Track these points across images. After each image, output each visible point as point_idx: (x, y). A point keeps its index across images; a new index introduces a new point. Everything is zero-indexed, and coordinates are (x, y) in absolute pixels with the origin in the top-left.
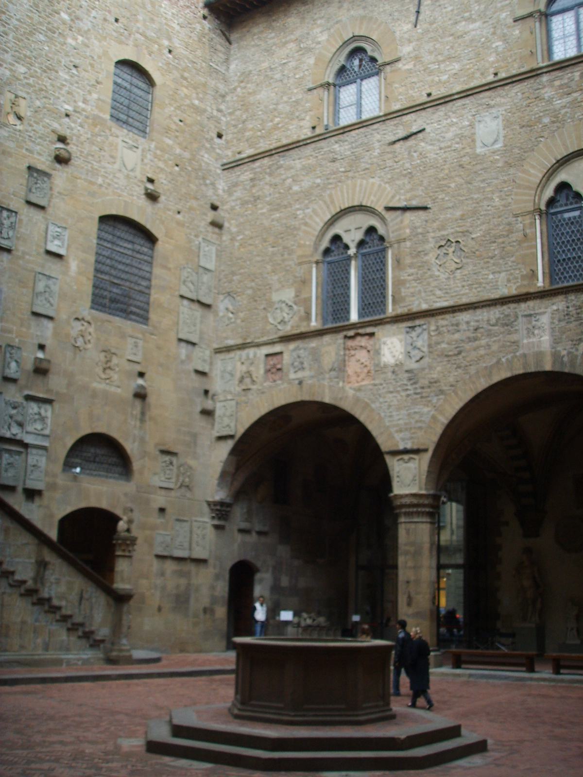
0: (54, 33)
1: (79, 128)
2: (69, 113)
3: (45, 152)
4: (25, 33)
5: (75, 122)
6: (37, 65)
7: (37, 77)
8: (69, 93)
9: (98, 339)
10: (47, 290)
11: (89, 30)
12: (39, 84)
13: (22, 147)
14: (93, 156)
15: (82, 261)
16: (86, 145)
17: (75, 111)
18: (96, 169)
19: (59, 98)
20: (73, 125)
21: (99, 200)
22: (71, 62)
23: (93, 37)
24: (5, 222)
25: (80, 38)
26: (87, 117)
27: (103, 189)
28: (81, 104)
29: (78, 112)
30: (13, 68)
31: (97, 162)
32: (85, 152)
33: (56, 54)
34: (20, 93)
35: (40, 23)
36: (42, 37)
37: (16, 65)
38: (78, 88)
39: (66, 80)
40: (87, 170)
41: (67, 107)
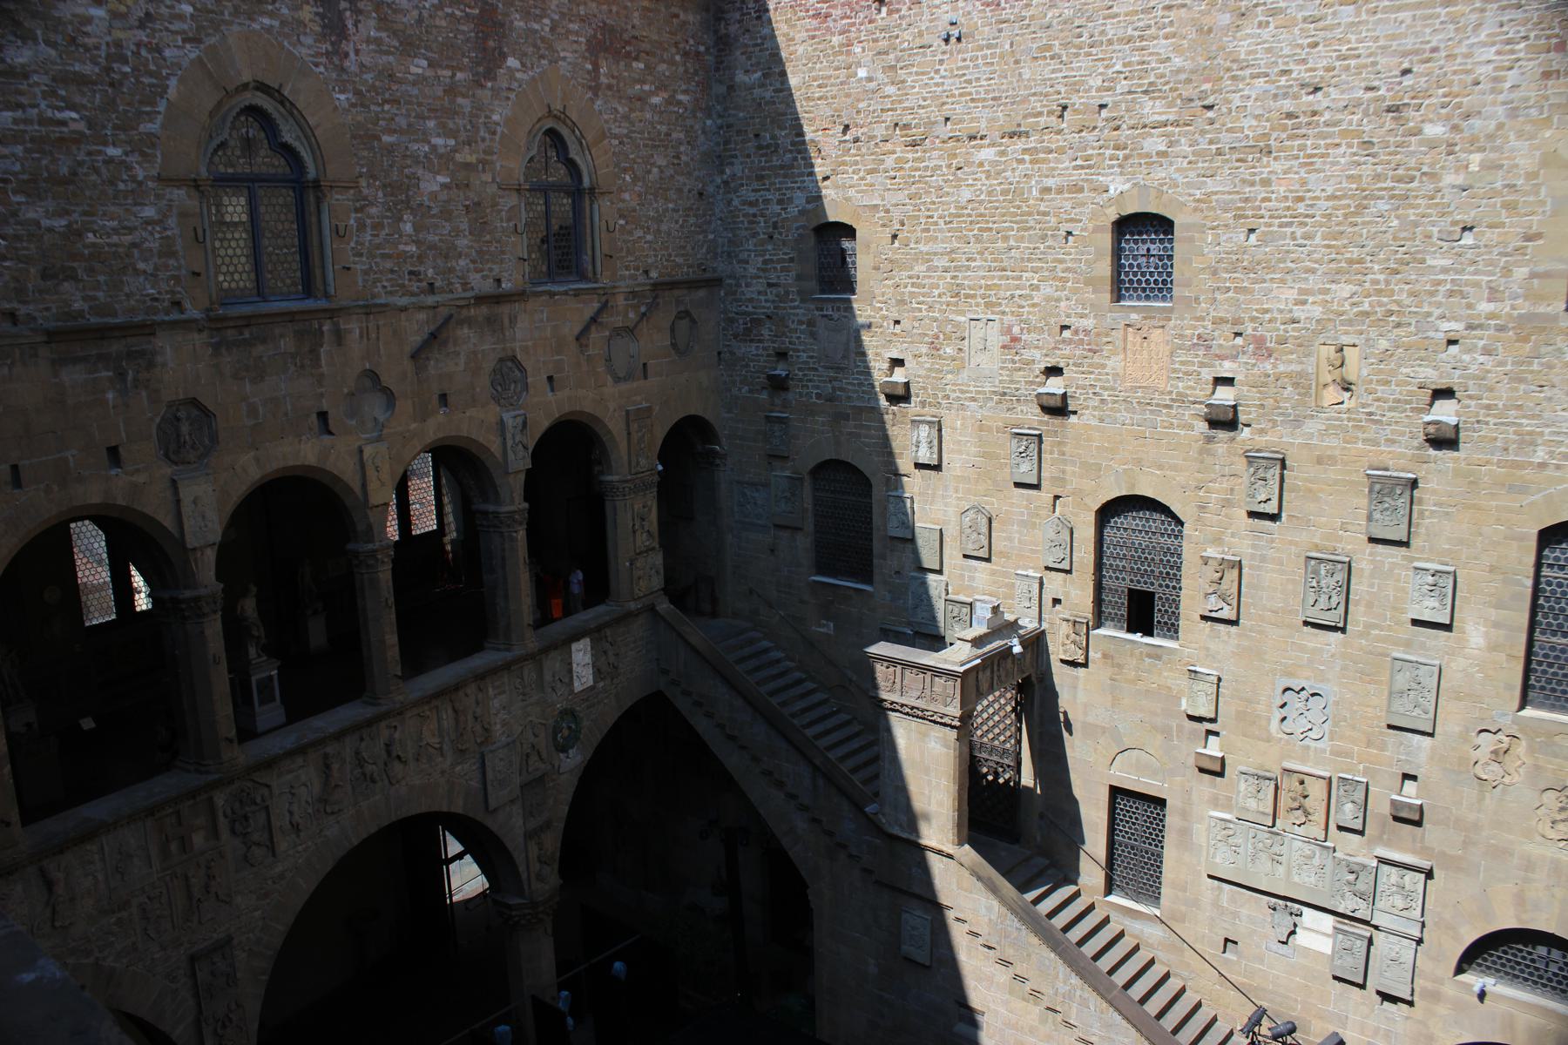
0: (1412, 180)
1: (1482, 359)
2: (1452, 336)
3: (1403, 434)
4: (1346, 216)
5: (1469, 351)
6: (1376, 267)
7: (1379, 292)
8: (1451, 293)
9: (1537, 767)
10: (1414, 686)
11: (1500, 126)
12: (1380, 304)
13: (1355, 440)
14: (1519, 407)
15: (1496, 625)
16: (1503, 390)
17: (1470, 327)
18: (1530, 433)
19: (1429, 314)
20: (1466, 358)
21: (1538, 497)
22: (1454, 223)
23: (1512, 136)
24: (1323, 583)
25: (1476, 158)
26: (1501, 329)
27: (1550, 472)
28: (1485, 307)
29: (1480, 326)
30: (1328, 298)
31: (1533, 417)
32: (1501, 405)
33: (1416, 224)
34: (1345, 340)
35: (1378, 177)
36: (1383, 206)
37: (1333, 286)
38: (1476, 273)
39: (1445, 270)
40: (1506, 441)
41: (1446, 326)
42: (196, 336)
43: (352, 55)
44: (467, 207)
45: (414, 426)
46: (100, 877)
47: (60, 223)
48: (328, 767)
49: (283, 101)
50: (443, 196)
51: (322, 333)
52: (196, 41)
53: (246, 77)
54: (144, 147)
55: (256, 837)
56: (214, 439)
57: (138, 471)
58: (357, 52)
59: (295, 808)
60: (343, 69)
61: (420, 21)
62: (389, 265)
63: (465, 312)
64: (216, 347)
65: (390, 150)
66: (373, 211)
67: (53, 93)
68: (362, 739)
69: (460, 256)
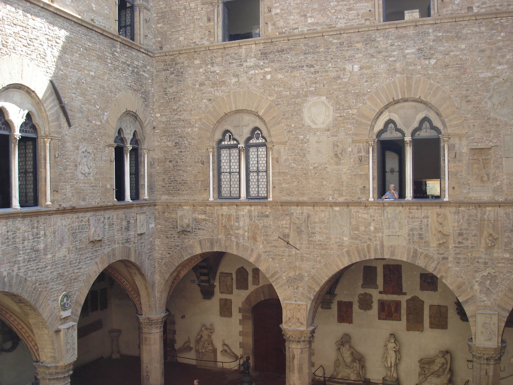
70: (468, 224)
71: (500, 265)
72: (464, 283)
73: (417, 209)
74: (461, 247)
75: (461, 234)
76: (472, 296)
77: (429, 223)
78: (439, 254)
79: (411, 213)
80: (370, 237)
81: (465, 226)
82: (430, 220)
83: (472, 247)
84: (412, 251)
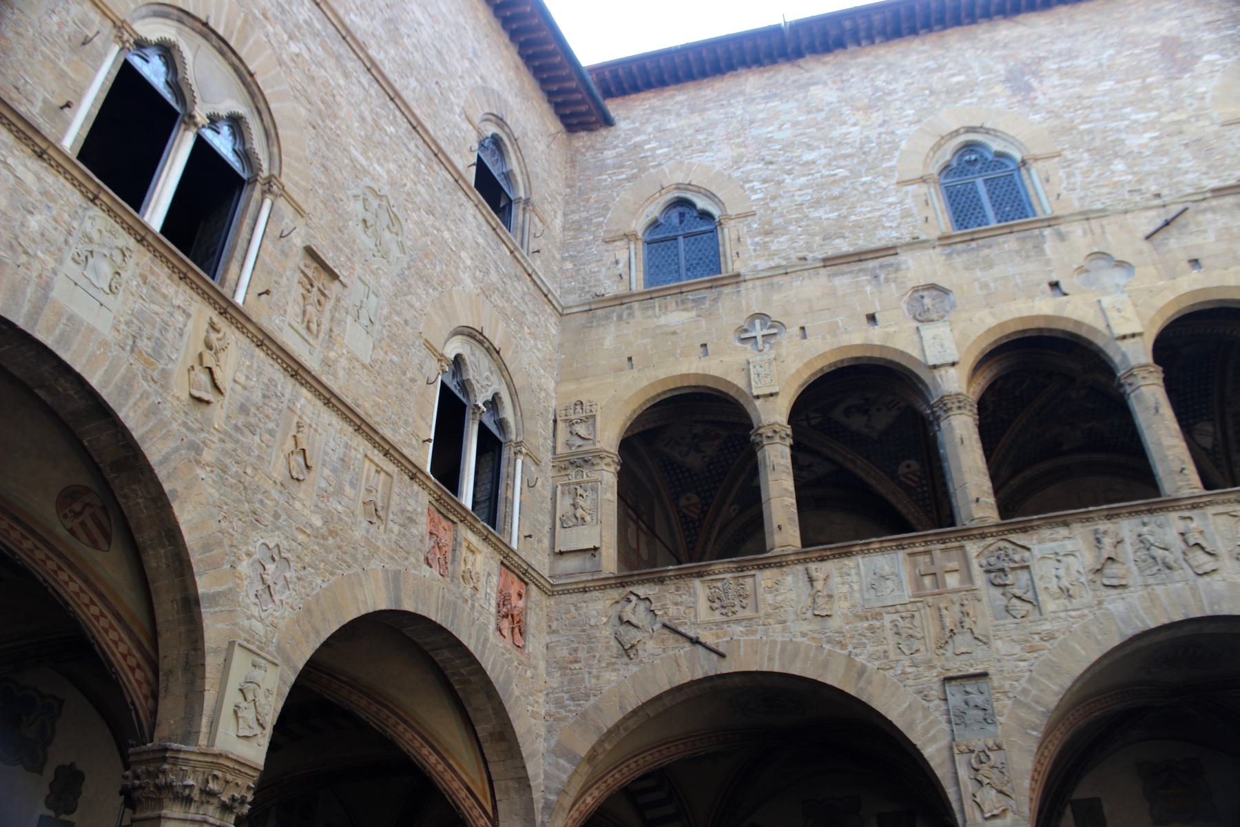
42: (931, 251)
43: (1041, 97)
44: (1186, 145)
45: (1161, 283)
46: (856, 587)
47: (834, 215)
48: (1098, 540)
49: (988, 132)
50: (1156, 143)
51: (1043, 237)
52: (919, 121)
53: (955, 127)
54: (887, 174)
55: (1018, 592)
56: (953, 306)
57: (890, 325)
58: (1045, 94)
59: (1061, 572)
60: (1034, 105)
61: (1100, 65)
62: (1105, 190)
63: (1204, 205)
64: (949, 255)
65: (1090, 132)
66: (1081, 165)
67: (829, 164)
68: (1144, 524)
69: (1187, 172)
70: (264, 396)
71: (301, 537)
72: (220, 543)
73: (170, 278)
74: (237, 441)
75: (243, 409)
76: (230, 589)
77: (186, 330)
78: (185, 424)
79: (153, 272)
80: (14, 243)
81: (257, 396)
82: (190, 324)
83: (259, 457)
84: (123, 370)
